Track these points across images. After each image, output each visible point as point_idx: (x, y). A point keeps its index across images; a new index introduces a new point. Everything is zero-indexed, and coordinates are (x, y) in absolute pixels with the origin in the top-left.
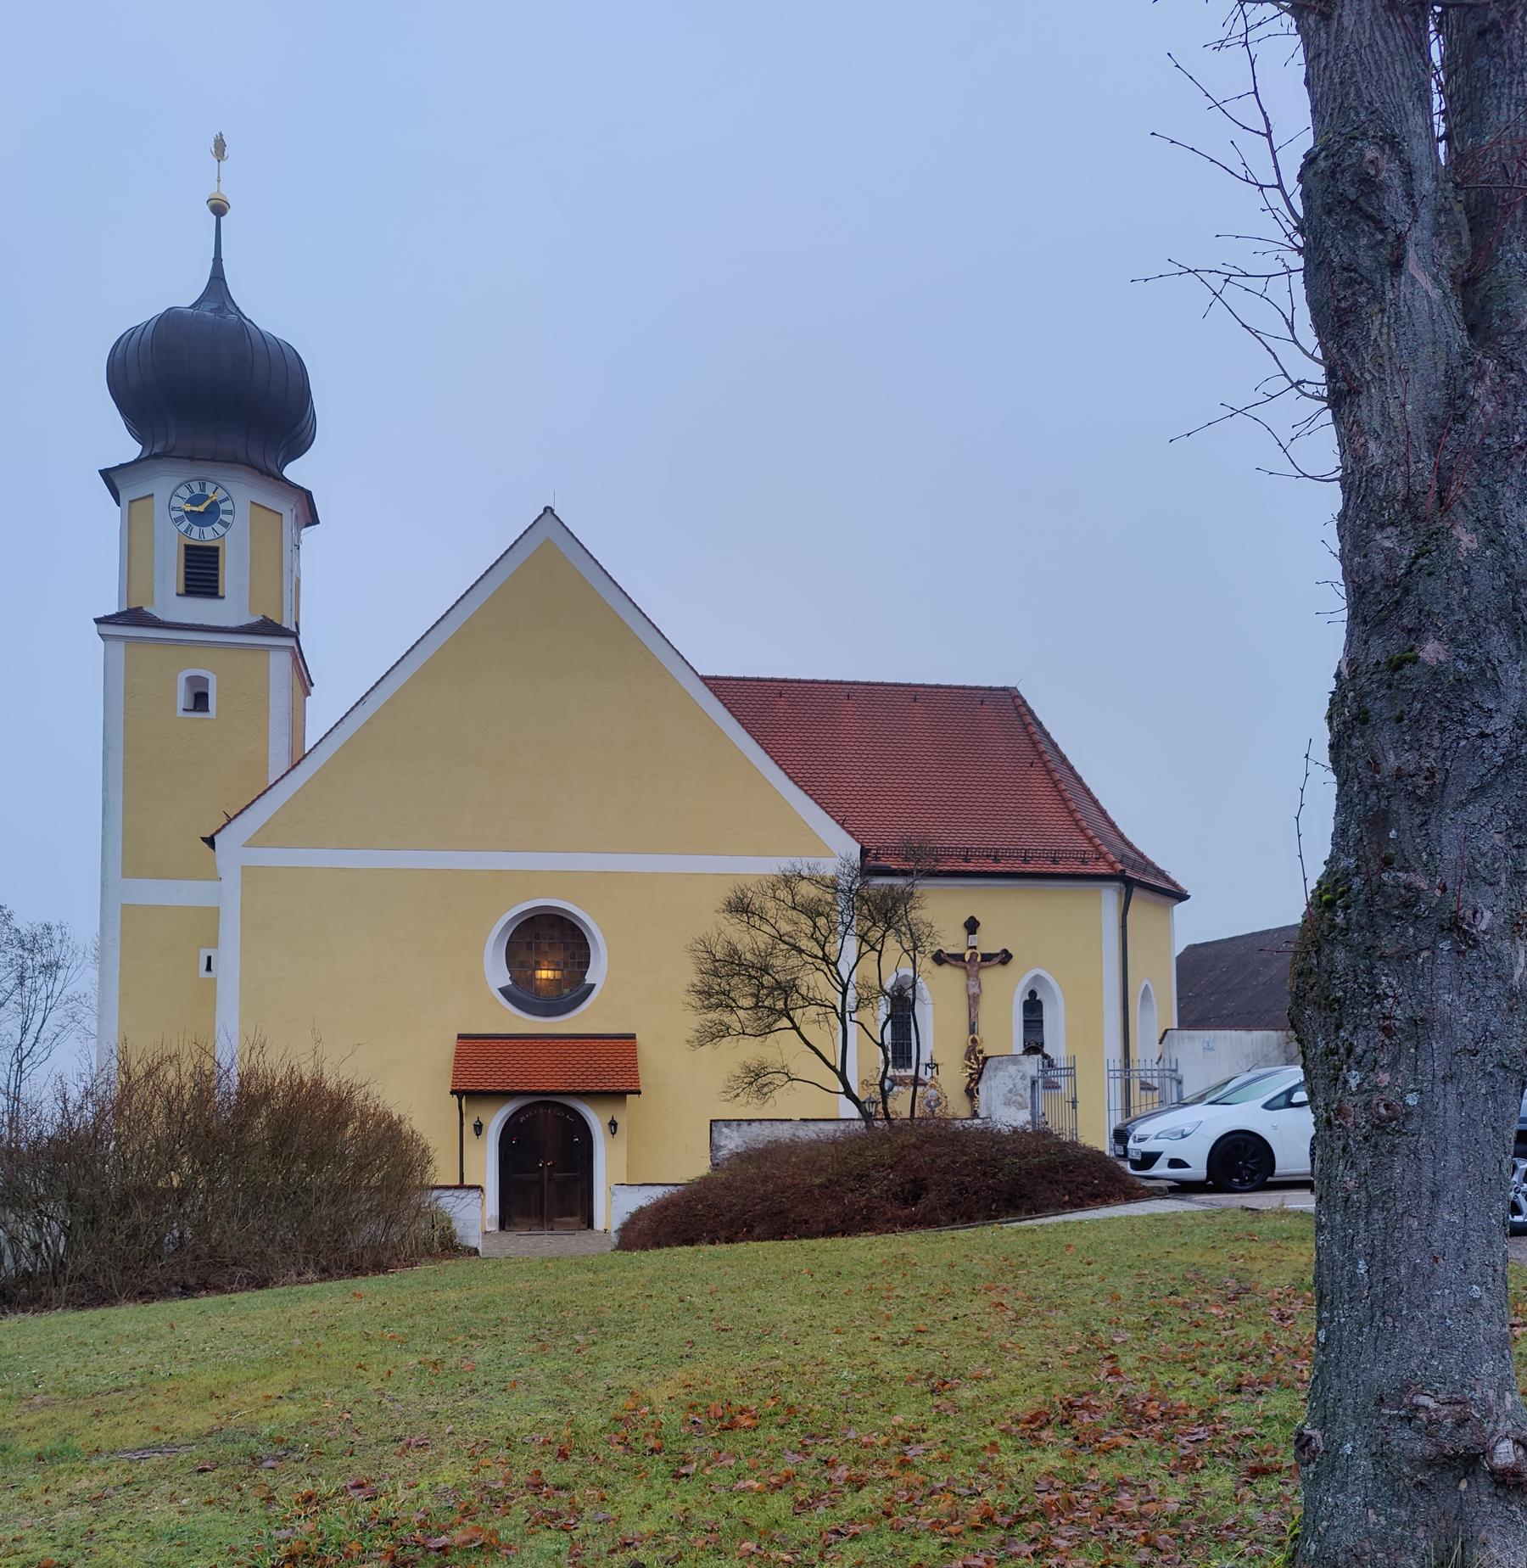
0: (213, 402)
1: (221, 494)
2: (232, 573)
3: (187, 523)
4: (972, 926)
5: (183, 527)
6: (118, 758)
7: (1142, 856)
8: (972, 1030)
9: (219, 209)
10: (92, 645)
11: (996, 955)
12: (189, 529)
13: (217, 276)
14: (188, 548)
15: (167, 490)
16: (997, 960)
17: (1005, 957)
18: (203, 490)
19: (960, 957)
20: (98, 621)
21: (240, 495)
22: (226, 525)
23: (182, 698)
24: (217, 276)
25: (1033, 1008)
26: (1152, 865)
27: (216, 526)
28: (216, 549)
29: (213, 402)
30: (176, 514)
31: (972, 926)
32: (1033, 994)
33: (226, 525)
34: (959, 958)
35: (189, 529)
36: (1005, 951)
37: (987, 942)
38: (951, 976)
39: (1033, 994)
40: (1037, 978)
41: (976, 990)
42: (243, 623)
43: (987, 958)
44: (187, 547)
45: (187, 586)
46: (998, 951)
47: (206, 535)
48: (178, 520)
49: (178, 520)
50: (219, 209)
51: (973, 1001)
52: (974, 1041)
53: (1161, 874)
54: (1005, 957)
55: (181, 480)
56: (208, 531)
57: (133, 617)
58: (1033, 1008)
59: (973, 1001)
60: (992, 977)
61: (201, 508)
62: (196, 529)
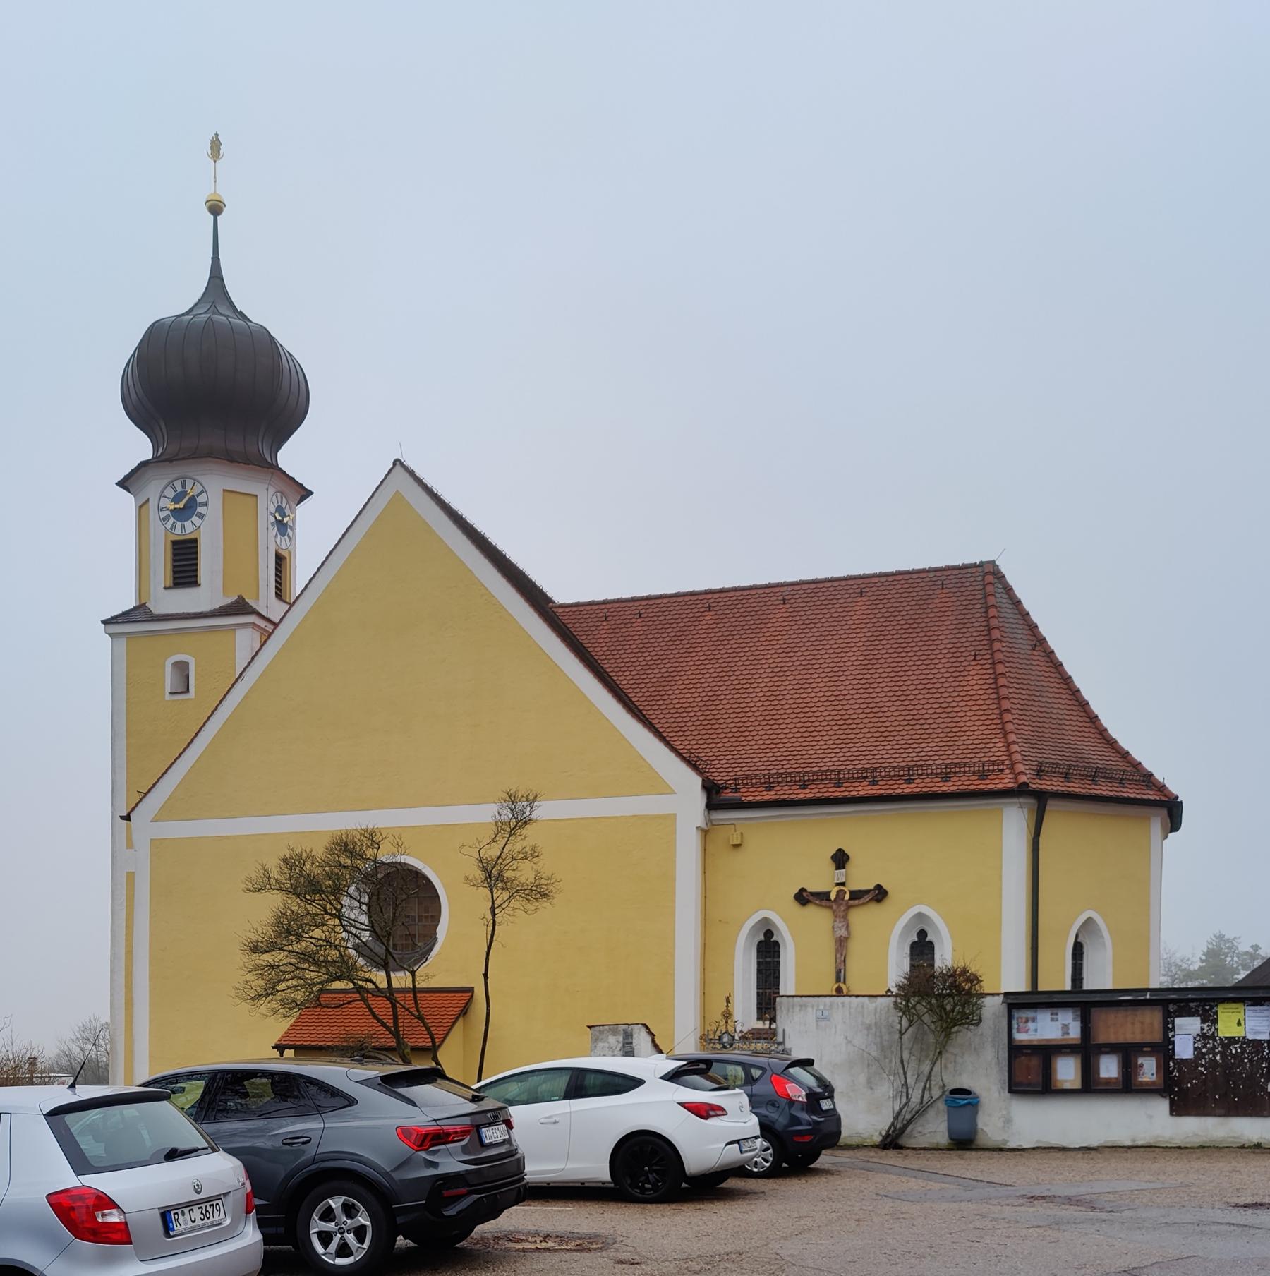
0: (213, 396)
1: (198, 488)
2: (209, 563)
3: (172, 519)
4: (841, 860)
5: (169, 525)
6: (123, 743)
7: (1125, 755)
9: (216, 209)
10: (103, 643)
11: (867, 892)
12: (174, 525)
14: (174, 543)
15: (158, 489)
16: (867, 898)
17: (880, 894)
18: (184, 487)
21: (214, 486)
22: (201, 516)
23: (169, 680)
26: (1137, 765)
27: (195, 519)
28: (195, 541)
29: (213, 396)
30: (163, 514)
31: (841, 860)
32: (922, 934)
33: (201, 516)
34: (823, 897)
35: (174, 525)
36: (879, 887)
37: (860, 877)
38: (818, 917)
39: (922, 934)
41: (843, 933)
42: (217, 606)
43: (856, 895)
44: (174, 543)
45: (175, 578)
46: (872, 887)
47: (185, 529)
48: (166, 519)
49: (166, 519)
50: (216, 209)
51: (842, 944)
53: (1148, 779)
54: (880, 894)
55: (165, 482)
56: (188, 524)
57: (140, 613)
59: (842, 944)
60: (863, 918)
61: (181, 505)
62: (179, 524)
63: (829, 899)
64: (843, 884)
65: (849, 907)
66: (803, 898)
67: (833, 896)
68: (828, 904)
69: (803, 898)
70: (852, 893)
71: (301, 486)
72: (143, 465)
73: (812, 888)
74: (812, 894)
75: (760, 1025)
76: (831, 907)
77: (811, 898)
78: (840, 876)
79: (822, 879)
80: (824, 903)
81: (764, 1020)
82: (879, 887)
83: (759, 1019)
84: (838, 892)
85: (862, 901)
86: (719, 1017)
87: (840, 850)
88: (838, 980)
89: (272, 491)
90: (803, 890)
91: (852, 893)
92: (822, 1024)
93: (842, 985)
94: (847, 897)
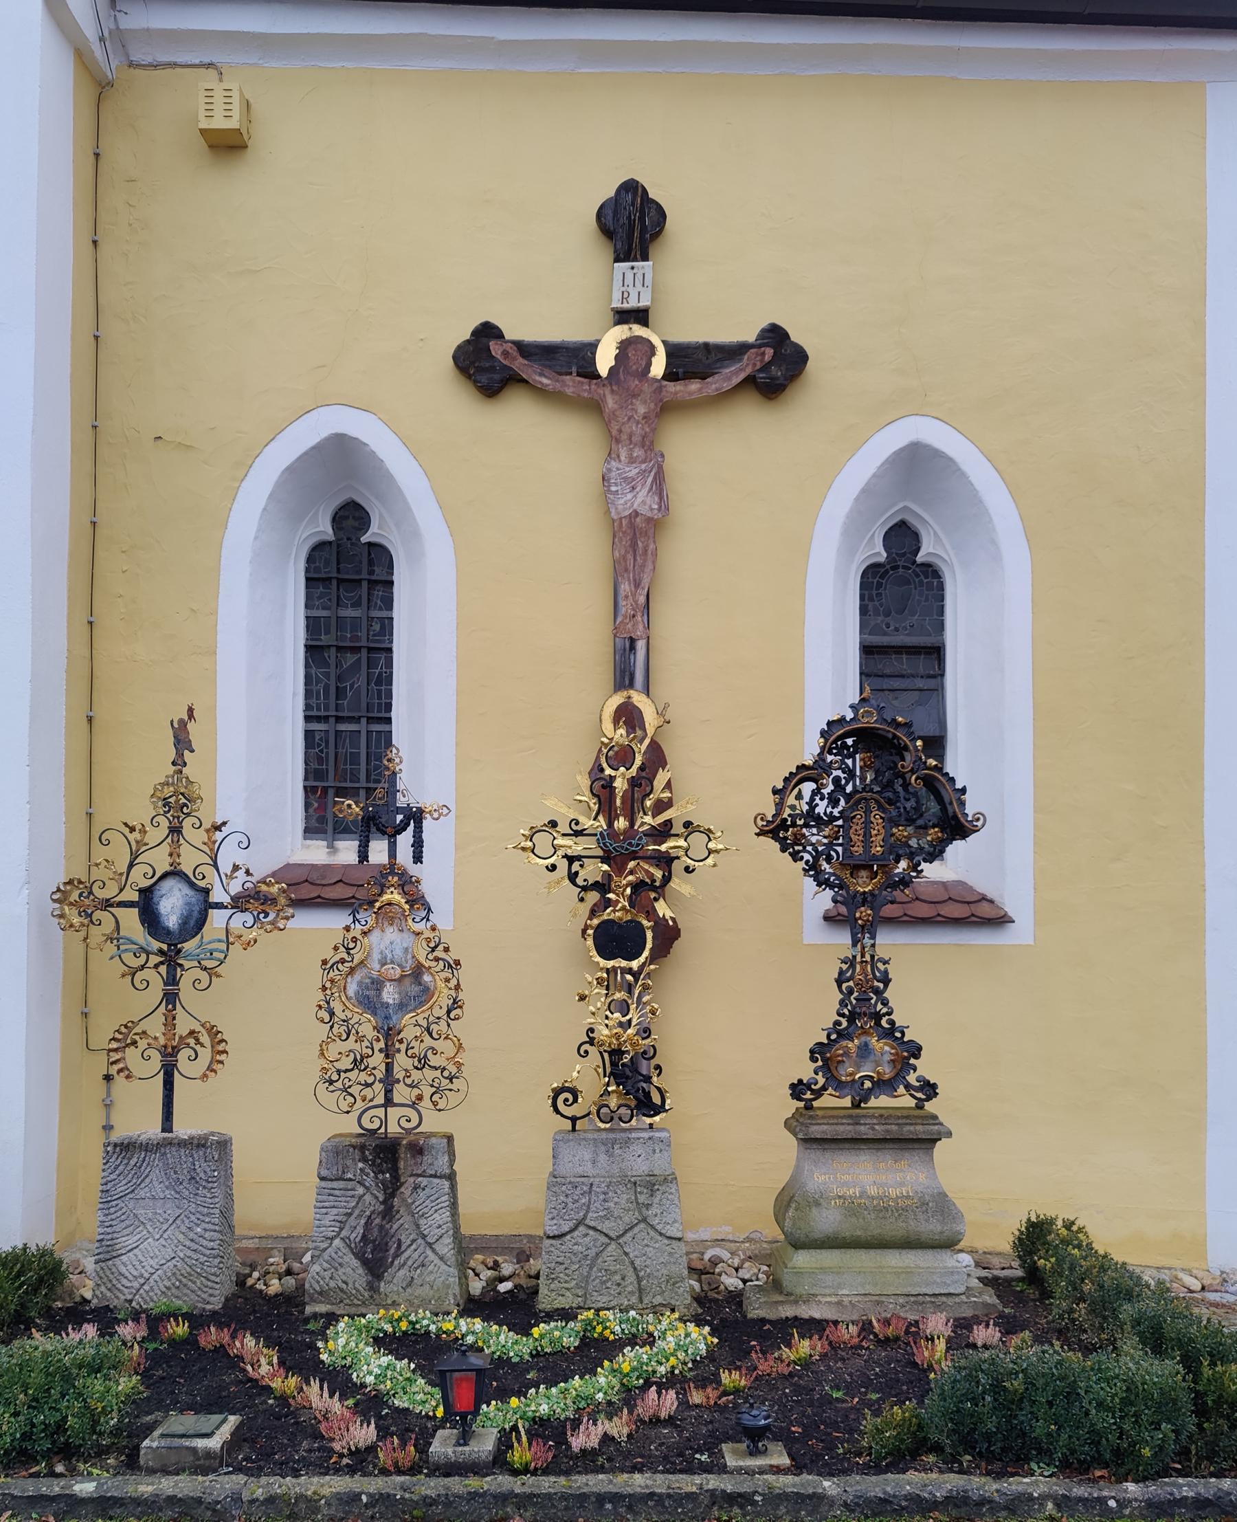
4: (632, 224)
8: (627, 669)
11: (734, 352)
16: (733, 374)
17: (776, 366)
19: (576, 358)
25: (902, 596)
31: (632, 224)
32: (902, 536)
36: (775, 335)
37: (705, 295)
38: (546, 446)
39: (902, 536)
40: (917, 464)
41: (642, 500)
43: (690, 362)
46: (750, 337)
51: (635, 544)
52: (628, 716)
54: (776, 366)
58: (902, 596)
59: (635, 544)
60: (716, 453)
63: (591, 374)
64: (640, 316)
65: (666, 409)
66: (488, 364)
67: (605, 361)
68: (585, 388)
69: (488, 364)
70: (676, 353)
73: (524, 324)
74: (525, 349)
75: (316, 853)
76: (594, 407)
77: (519, 364)
78: (633, 283)
79: (561, 294)
80: (572, 384)
81: (341, 829)
82: (775, 335)
83: (320, 823)
84: (625, 347)
86: (141, 810)
87: (631, 188)
88: (624, 678)
90: (487, 332)
91: (676, 353)
93: (639, 699)
94: (658, 367)
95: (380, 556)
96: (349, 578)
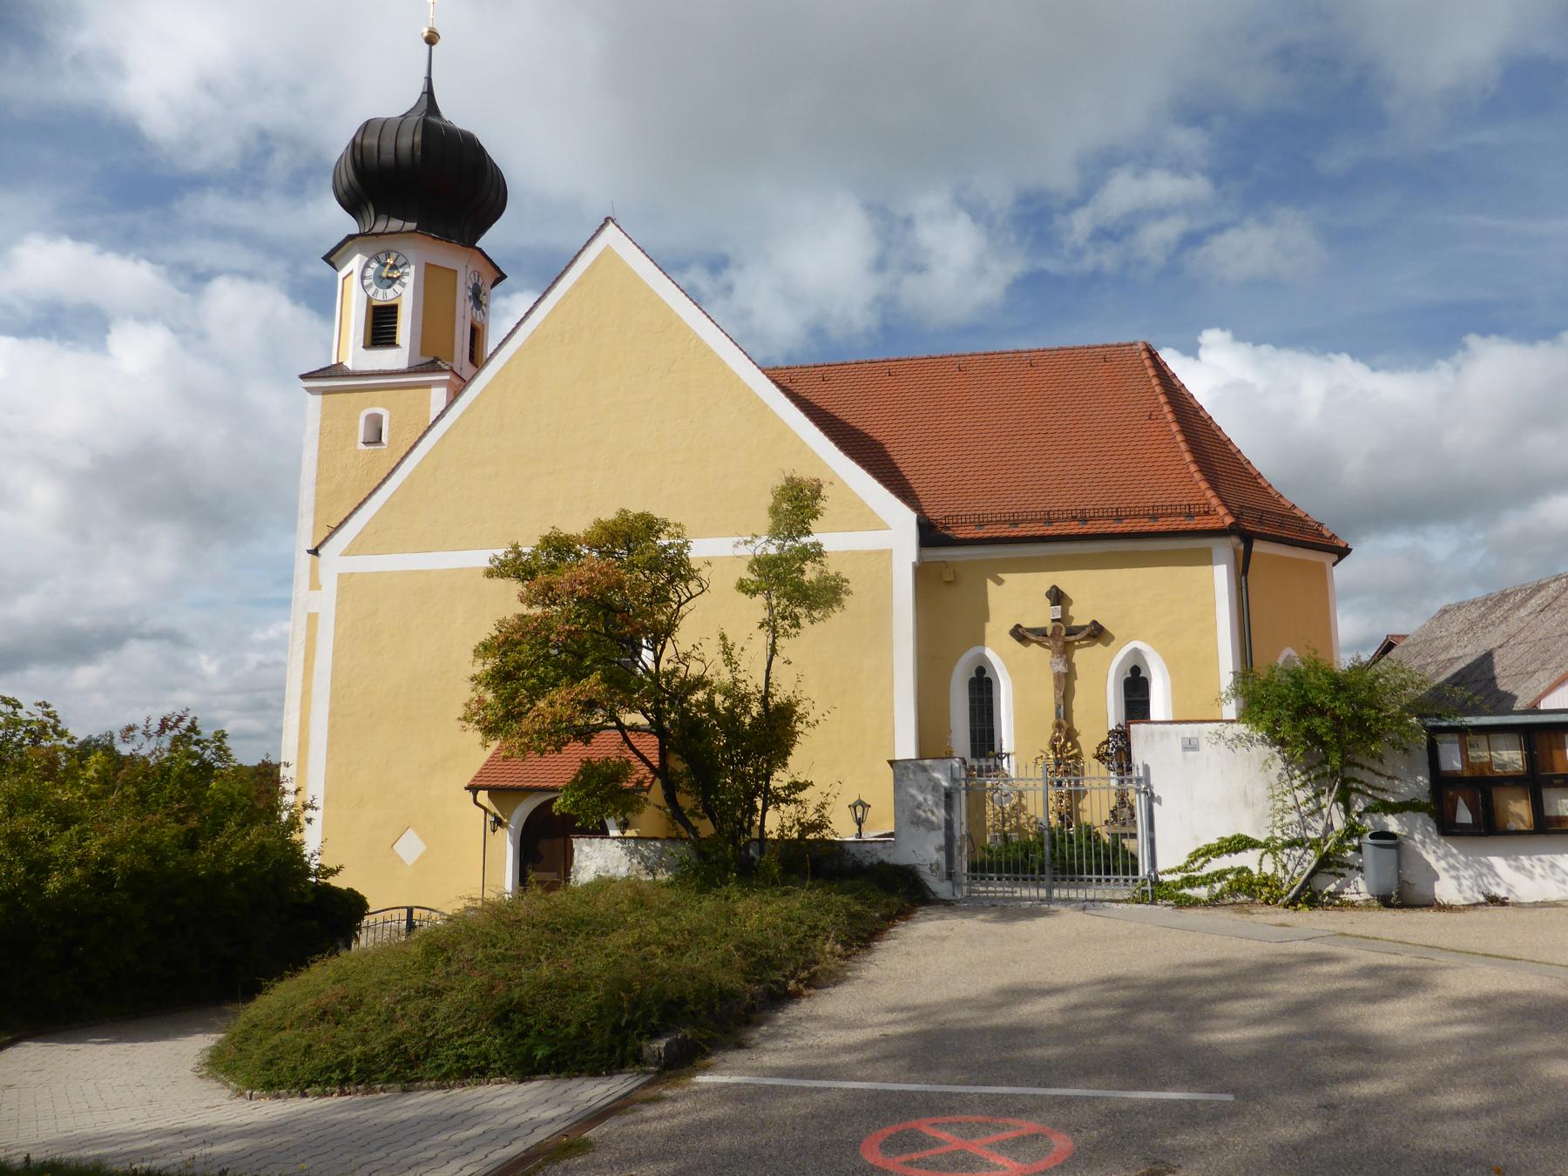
11: (1083, 628)
12: (376, 292)
13: (429, 92)
20: (303, 377)
24: (429, 92)
27: (396, 287)
35: (376, 292)
36: (1094, 622)
47: (384, 296)
50: (431, 39)
60: (1082, 656)
71: (497, 269)
72: (351, 237)
74: (1028, 630)
85: (1079, 637)
88: (1058, 715)
89: (470, 270)
90: (1018, 626)
92: (1191, 754)
95: (989, 681)
96: (982, 687)
